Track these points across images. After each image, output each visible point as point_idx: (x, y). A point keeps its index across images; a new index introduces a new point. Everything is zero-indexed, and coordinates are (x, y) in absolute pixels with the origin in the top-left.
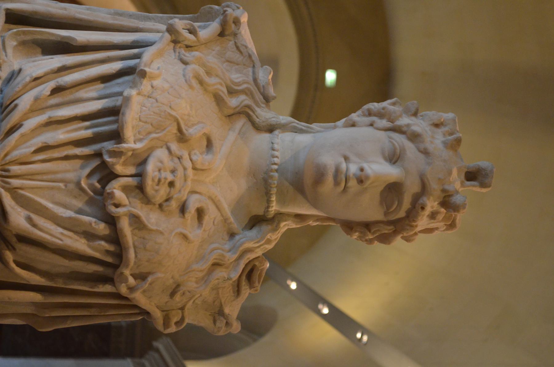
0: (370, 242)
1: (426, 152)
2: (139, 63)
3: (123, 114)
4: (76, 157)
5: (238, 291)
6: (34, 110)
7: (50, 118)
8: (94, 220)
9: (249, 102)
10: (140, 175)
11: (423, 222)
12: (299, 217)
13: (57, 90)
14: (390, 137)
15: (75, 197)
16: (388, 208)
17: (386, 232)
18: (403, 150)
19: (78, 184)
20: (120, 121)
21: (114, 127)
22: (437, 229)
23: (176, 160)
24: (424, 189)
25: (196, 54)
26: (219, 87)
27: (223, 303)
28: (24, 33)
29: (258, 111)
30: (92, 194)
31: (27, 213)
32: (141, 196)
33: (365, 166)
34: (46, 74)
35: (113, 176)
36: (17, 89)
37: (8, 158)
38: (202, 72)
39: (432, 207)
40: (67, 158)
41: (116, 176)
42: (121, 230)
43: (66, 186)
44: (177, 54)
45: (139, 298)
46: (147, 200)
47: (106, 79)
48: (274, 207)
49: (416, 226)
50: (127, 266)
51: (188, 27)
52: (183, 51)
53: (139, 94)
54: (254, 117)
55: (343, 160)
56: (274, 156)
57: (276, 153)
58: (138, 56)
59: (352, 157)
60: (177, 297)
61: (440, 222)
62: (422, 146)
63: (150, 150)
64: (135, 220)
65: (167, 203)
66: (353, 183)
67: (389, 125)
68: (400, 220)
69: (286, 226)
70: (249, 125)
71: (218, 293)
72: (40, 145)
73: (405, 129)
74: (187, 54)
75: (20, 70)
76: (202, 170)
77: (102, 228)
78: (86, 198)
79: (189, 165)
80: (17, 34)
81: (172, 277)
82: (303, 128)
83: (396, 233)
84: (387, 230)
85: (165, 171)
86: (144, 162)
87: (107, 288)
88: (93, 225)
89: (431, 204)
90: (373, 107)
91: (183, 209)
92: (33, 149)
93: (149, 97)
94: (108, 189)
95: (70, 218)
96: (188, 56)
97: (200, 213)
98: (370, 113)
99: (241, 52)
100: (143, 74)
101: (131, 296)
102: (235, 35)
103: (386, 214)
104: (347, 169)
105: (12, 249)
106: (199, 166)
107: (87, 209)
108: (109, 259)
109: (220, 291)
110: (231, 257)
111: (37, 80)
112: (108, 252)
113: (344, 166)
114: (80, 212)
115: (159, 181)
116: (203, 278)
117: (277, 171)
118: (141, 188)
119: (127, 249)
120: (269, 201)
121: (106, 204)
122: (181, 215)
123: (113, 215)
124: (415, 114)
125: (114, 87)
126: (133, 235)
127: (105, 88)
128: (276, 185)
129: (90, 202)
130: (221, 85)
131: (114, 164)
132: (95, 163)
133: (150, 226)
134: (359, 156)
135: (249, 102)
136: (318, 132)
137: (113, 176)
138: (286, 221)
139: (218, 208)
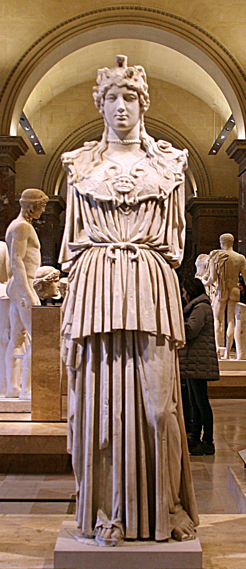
3: (102, 200)
9: (97, 152)
10: (124, 194)
12: (141, 130)
16: (133, 98)
21: (107, 204)
27: (173, 158)
28: (76, 236)
29: (101, 148)
32: (131, 193)
37: (120, 240)
41: (124, 202)
45: (169, 191)
50: (156, 197)
58: (82, 196)
59: (115, 114)
67: (102, 99)
70: (106, 152)
75: (89, 237)
76: (122, 170)
77: (143, 206)
81: (161, 179)
84: (142, 97)
86: (119, 192)
87: (166, 203)
94: (129, 205)
98: (99, 106)
99: (79, 156)
101: (168, 194)
103: (136, 99)
105: (152, 236)
107: (136, 212)
108: (154, 203)
109: (169, 160)
112: (152, 203)
125: (93, 204)
131: (120, 203)
134: (114, 111)
135: (97, 152)
138: (142, 135)
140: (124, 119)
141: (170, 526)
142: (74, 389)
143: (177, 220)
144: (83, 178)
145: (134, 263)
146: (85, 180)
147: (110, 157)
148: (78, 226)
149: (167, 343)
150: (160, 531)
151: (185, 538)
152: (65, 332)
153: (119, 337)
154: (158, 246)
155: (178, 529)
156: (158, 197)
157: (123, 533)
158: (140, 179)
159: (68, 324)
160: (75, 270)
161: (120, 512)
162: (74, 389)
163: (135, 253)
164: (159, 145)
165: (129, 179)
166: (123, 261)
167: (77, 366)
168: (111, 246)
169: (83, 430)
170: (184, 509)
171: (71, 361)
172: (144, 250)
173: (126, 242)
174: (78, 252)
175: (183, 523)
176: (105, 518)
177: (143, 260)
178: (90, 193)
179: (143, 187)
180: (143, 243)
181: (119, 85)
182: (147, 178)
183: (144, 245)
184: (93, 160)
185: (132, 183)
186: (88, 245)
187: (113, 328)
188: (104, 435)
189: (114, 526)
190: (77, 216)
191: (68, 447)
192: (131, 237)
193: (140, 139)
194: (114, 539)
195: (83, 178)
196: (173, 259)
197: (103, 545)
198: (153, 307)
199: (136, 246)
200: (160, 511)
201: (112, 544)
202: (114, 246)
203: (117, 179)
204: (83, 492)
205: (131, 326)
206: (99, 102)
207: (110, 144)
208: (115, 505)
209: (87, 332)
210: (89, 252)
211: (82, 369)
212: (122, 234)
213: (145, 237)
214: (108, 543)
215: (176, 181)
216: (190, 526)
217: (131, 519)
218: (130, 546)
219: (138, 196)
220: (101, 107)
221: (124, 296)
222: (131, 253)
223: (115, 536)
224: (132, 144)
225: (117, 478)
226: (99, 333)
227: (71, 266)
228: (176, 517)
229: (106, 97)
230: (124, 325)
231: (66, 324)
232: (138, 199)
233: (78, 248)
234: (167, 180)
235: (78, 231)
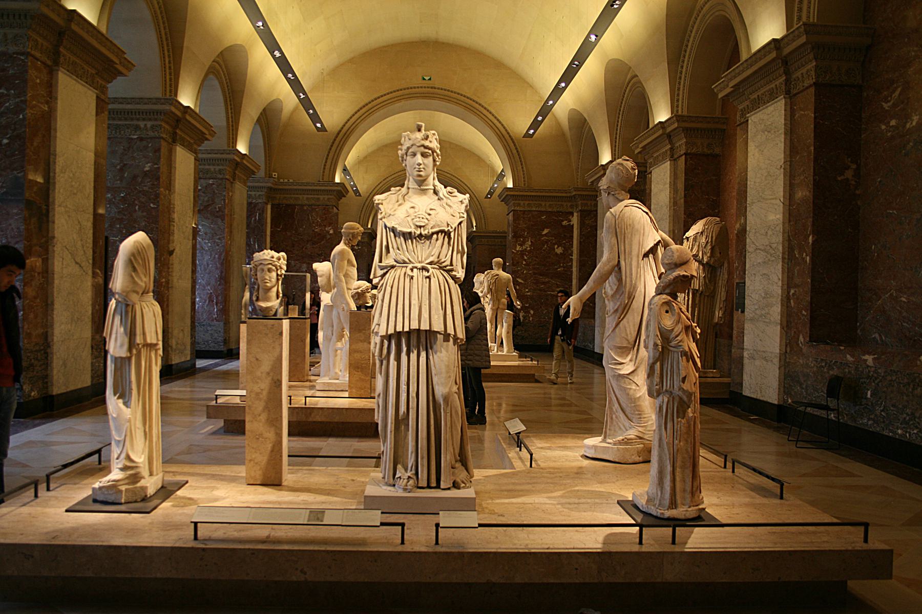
9: (400, 196)
10: (420, 227)
12: (434, 179)
41: (421, 234)
45: (455, 225)
58: (389, 228)
67: (405, 156)
77: (435, 236)
84: (435, 154)
86: (417, 226)
87: (452, 234)
98: (402, 161)
101: (454, 228)
108: (443, 234)
112: (441, 234)
125: (397, 234)
135: (400, 196)
140: (421, 171)
141: (452, 477)
142: (381, 374)
143: (460, 248)
144: (390, 215)
145: (428, 280)
147: (410, 199)
149: (451, 340)
150: (444, 481)
151: (463, 487)
153: (416, 335)
154: (445, 267)
155: (458, 480)
156: (446, 230)
157: (416, 482)
158: (433, 216)
159: (377, 324)
160: (383, 284)
162: (381, 374)
163: (428, 272)
167: (383, 357)
168: (410, 266)
170: (462, 465)
171: (379, 353)
174: (386, 270)
175: (462, 476)
176: (403, 471)
178: (395, 226)
181: (418, 145)
183: (435, 266)
184: (398, 201)
185: (427, 219)
188: (403, 409)
191: (376, 417)
192: (425, 260)
194: (409, 487)
195: (390, 215)
198: (441, 312)
199: (429, 266)
205: (425, 326)
206: (402, 157)
207: (410, 190)
208: (411, 462)
209: (391, 331)
210: (394, 271)
213: (436, 260)
214: (405, 490)
215: (460, 218)
217: (422, 472)
218: (421, 492)
219: (431, 228)
223: (410, 485)
224: (427, 189)
225: (412, 441)
226: (400, 332)
227: (380, 281)
228: (456, 471)
229: (408, 154)
230: (419, 326)
232: (431, 231)
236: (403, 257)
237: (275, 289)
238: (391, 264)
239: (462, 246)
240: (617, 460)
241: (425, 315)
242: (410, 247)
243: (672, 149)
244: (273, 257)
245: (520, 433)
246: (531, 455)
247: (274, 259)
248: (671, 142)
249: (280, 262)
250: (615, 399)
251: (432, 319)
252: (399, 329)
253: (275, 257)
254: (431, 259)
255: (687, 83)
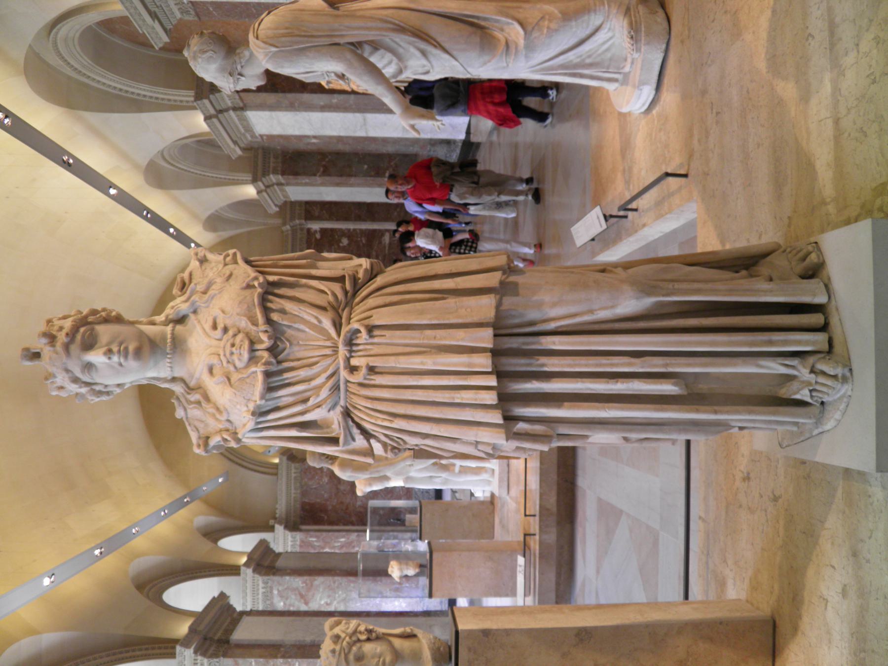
0: (104, 310)
1: (67, 371)
2: (256, 419)
3: (264, 389)
4: (293, 361)
5: (191, 275)
6: (320, 387)
7: (309, 384)
8: (280, 322)
9: (189, 397)
10: (252, 350)
11: (68, 324)
13: (306, 400)
14: (92, 379)
15: (292, 335)
16: (91, 334)
17: (92, 317)
18: (83, 372)
19: (291, 344)
20: (266, 384)
22: (60, 319)
23: (230, 361)
24: (67, 347)
25: (221, 426)
26: (207, 406)
27: (200, 268)
28: (328, 433)
29: (182, 391)
30: (282, 338)
31: (321, 326)
32: (252, 338)
33: (107, 361)
34: (313, 409)
35: (270, 350)
36: (329, 400)
37: (333, 358)
38: (218, 416)
39: (61, 335)
40: (299, 360)
42: (263, 316)
43: (298, 342)
44: (234, 426)
45: (251, 273)
46: (247, 335)
47: (277, 409)
48: (169, 329)
49: (72, 322)
50: (259, 293)
51: (228, 443)
52: (230, 428)
53: (256, 401)
54: (184, 387)
55: (123, 364)
56: (170, 363)
57: (169, 365)
59: (117, 366)
60: (228, 273)
61: (56, 325)
62: (70, 375)
63: (247, 366)
64: (255, 324)
65: (235, 333)
66: (115, 349)
67: (94, 387)
68: (83, 326)
69: (161, 318)
70: (188, 381)
71: (203, 274)
72: (314, 367)
73: (83, 385)
74: (228, 426)
75: (329, 411)
77: (275, 317)
78: (286, 335)
79: (222, 357)
80: (332, 432)
82: (152, 380)
83: (86, 317)
84: (91, 319)
85: (237, 354)
87: (271, 278)
88: (280, 319)
89: (62, 337)
90: (106, 397)
91: (226, 330)
92: (318, 365)
93: (249, 400)
94: (272, 342)
95: (295, 323)
96: (227, 425)
97: (215, 327)
98: (108, 393)
100: (253, 414)
102: (199, 438)
103: (93, 329)
104: (119, 358)
105: (329, 303)
106: (217, 357)
107: (285, 328)
108: (271, 297)
110: (195, 297)
111: (318, 406)
112: (271, 302)
113: (122, 360)
114: (289, 327)
115: (240, 348)
116: (212, 284)
117: (168, 354)
118: (252, 343)
119: (259, 304)
120: (173, 334)
121: (273, 332)
122: (227, 326)
123: (268, 326)
124: (77, 394)
125: (271, 404)
126: (256, 313)
127: (278, 403)
128: (168, 345)
129: (283, 333)
130: (205, 408)
131: (269, 357)
132: (281, 357)
133: (245, 318)
135: (189, 397)
136: (143, 379)
137: (270, 350)
138: (161, 321)
139: (204, 330)
143: (304, 261)
145: (376, 333)
146: (231, 419)
148: (312, 431)
149: (512, 278)
152: (491, 452)
154: (346, 293)
156: (259, 290)
158: (229, 322)
159: (476, 447)
160: (386, 436)
161: (787, 360)
163: (358, 331)
164: (179, 293)
165: (227, 341)
166: (372, 353)
167: (550, 432)
168: (344, 374)
169: (653, 421)
172: (352, 316)
173: (338, 347)
174: (356, 431)
176: (795, 385)
177: (371, 317)
179: (242, 317)
180: (341, 318)
182: (228, 309)
183: (345, 315)
184: (199, 403)
185: (235, 335)
186: (342, 413)
187: (490, 370)
188: (667, 388)
189: (812, 371)
190: (294, 433)
192: (330, 338)
193: (167, 325)
196: (368, 267)
197: (850, 389)
198: (451, 302)
199: (345, 330)
200: (785, 295)
201: (848, 374)
202: (345, 368)
203: (228, 362)
204: (740, 420)
205: (485, 338)
206: (100, 393)
208: (775, 367)
209: (496, 418)
210: (356, 412)
211: (553, 425)
212: (324, 353)
213: (331, 314)
215: (236, 262)
216: (790, 252)
217: (799, 343)
220: (109, 389)
221: (433, 351)
222: (357, 338)
225: (735, 365)
227: (379, 441)
231: (476, 451)
232: (263, 327)
233: (347, 429)
234: (234, 276)
235: (319, 431)
236: (324, 393)
237: (397, 643)
238: (340, 418)
239: (298, 258)
240: (664, 46)
241: (462, 338)
242: (303, 373)
243: (235, 109)
244: (333, 651)
245: (605, 216)
246: (668, 175)
247: (338, 648)
248: (227, 110)
249: (343, 635)
250: (562, 57)
251: (469, 320)
252: (491, 398)
253: (332, 646)
254: (327, 324)
255: (161, 90)
